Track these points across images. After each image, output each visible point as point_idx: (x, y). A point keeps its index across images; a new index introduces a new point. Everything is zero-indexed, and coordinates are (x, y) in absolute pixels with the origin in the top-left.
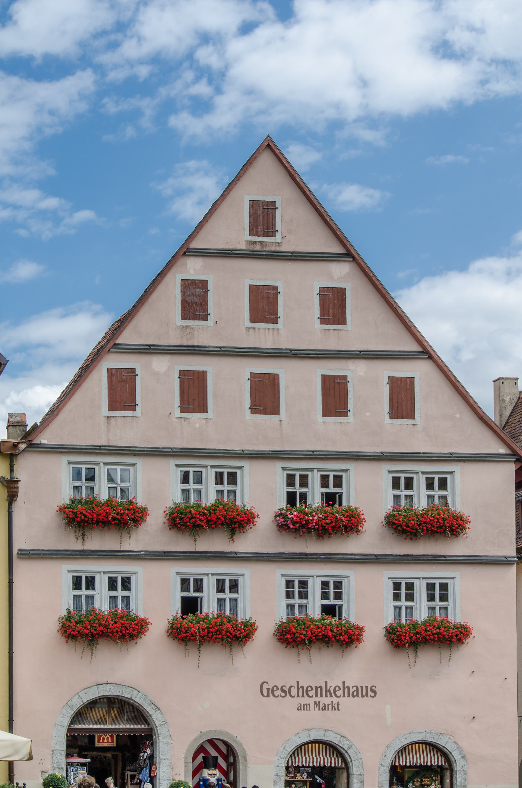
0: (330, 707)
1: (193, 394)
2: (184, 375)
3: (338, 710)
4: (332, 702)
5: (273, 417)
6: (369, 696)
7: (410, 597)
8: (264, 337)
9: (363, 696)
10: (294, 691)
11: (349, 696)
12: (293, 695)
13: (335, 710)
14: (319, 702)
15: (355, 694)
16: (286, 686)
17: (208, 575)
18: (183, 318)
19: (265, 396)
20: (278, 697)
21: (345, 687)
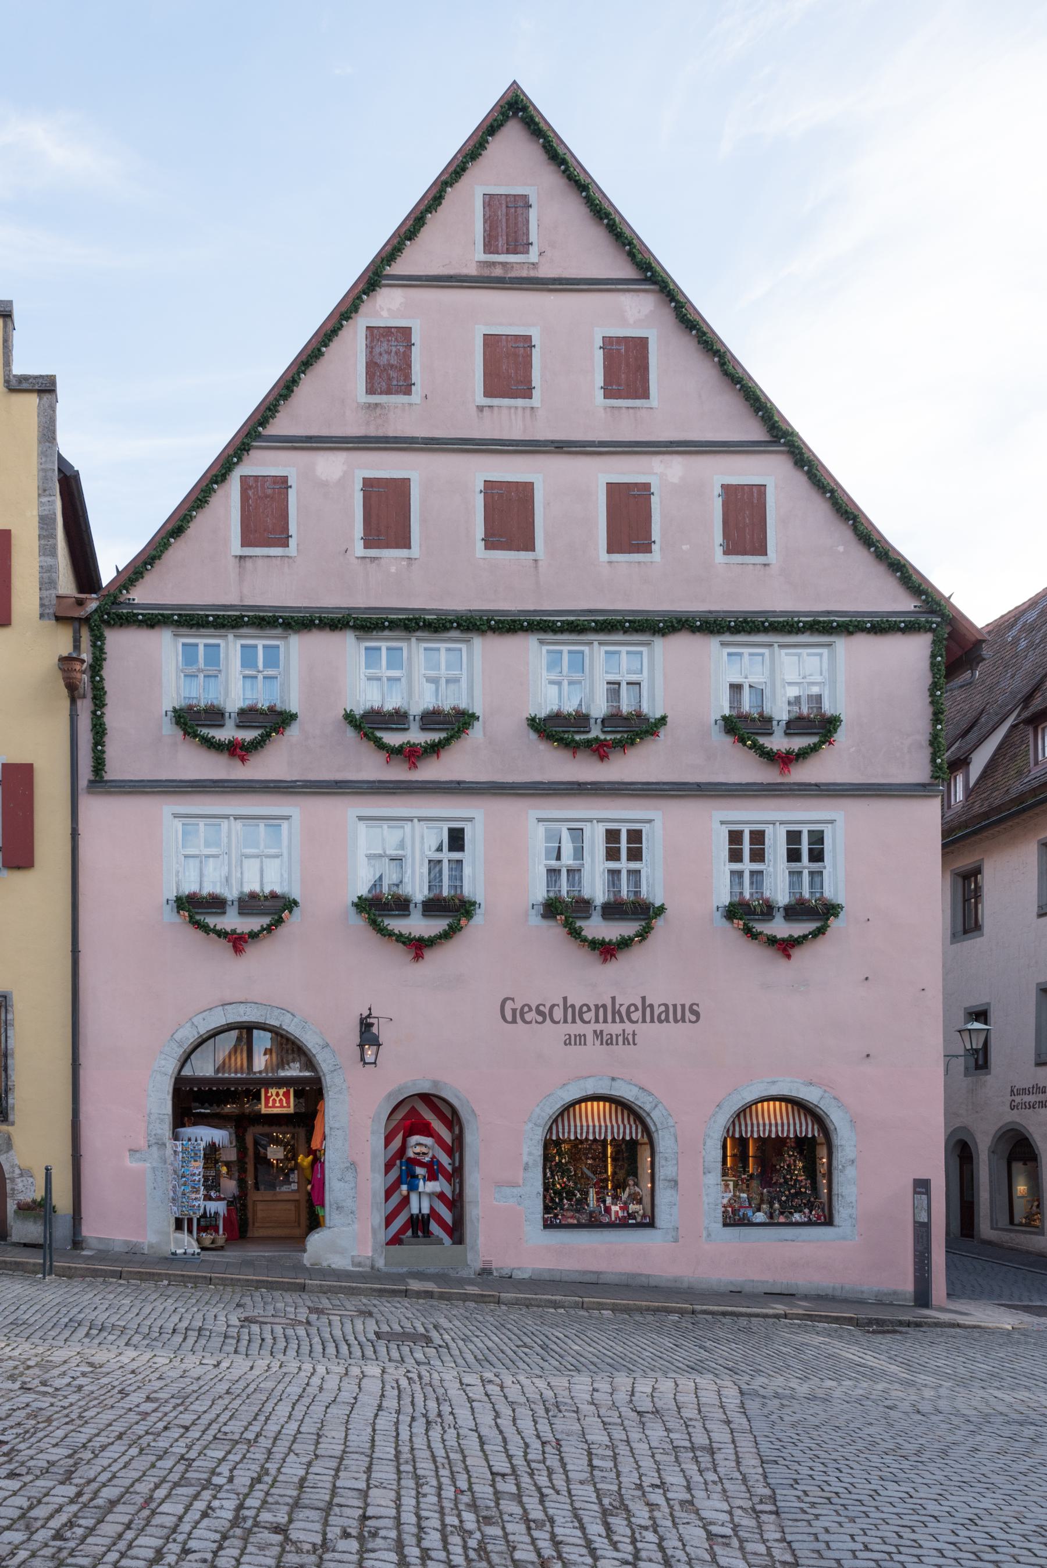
0: (620, 1039)
2: (369, 484)
3: (635, 1044)
5: (523, 555)
8: (509, 419)
9: (676, 1021)
10: (558, 1014)
11: (652, 1021)
12: (557, 1020)
13: (629, 1044)
14: (601, 1032)
15: (663, 1017)
18: (371, 391)
20: (530, 1022)
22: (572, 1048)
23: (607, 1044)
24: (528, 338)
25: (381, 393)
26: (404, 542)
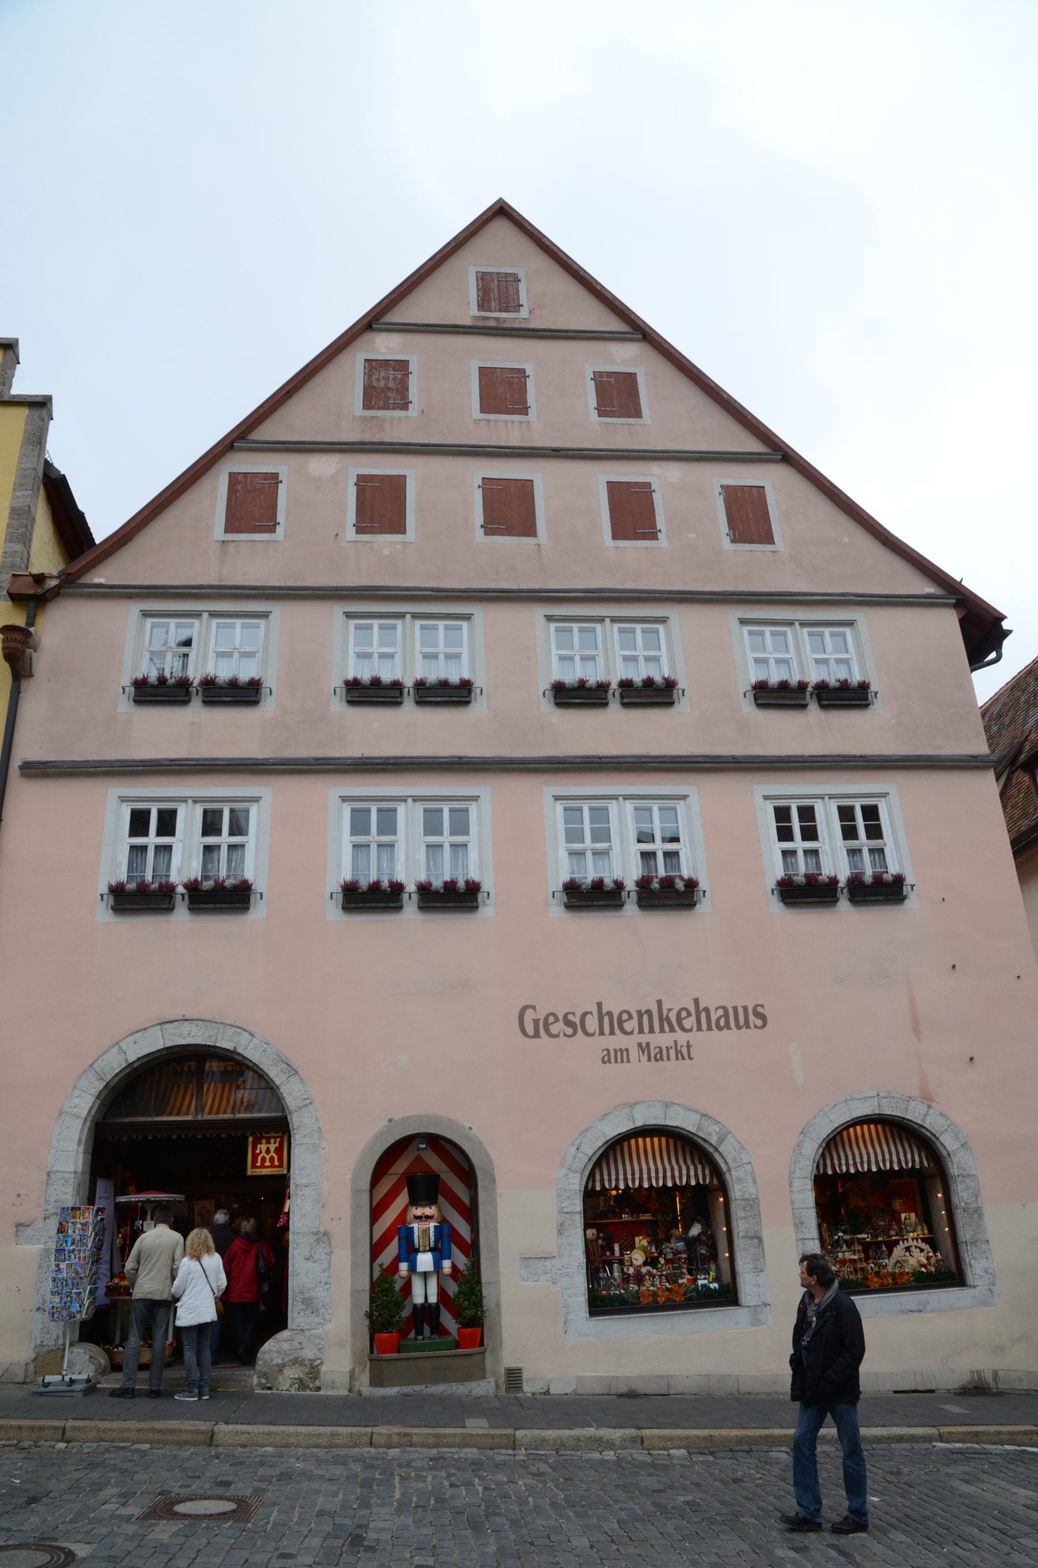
0: (672, 1052)
1: (381, 507)
2: (363, 481)
3: (691, 1058)
4: (676, 1042)
6: (752, 1025)
7: (810, 833)
9: (739, 1027)
11: (710, 1028)
12: (590, 1030)
13: (683, 1058)
14: (648, 1044)
15: (722, 1022)
16: (574, 1014)
17: (406, 801)
18: (367, 405)
19: (509, 511)
20: (557, 1036)
21: (700, 1010)
22: (613, 1067)
23: (656, 1060)
24: (523, 371)
25: (380, 408)
26: (399, 528)
